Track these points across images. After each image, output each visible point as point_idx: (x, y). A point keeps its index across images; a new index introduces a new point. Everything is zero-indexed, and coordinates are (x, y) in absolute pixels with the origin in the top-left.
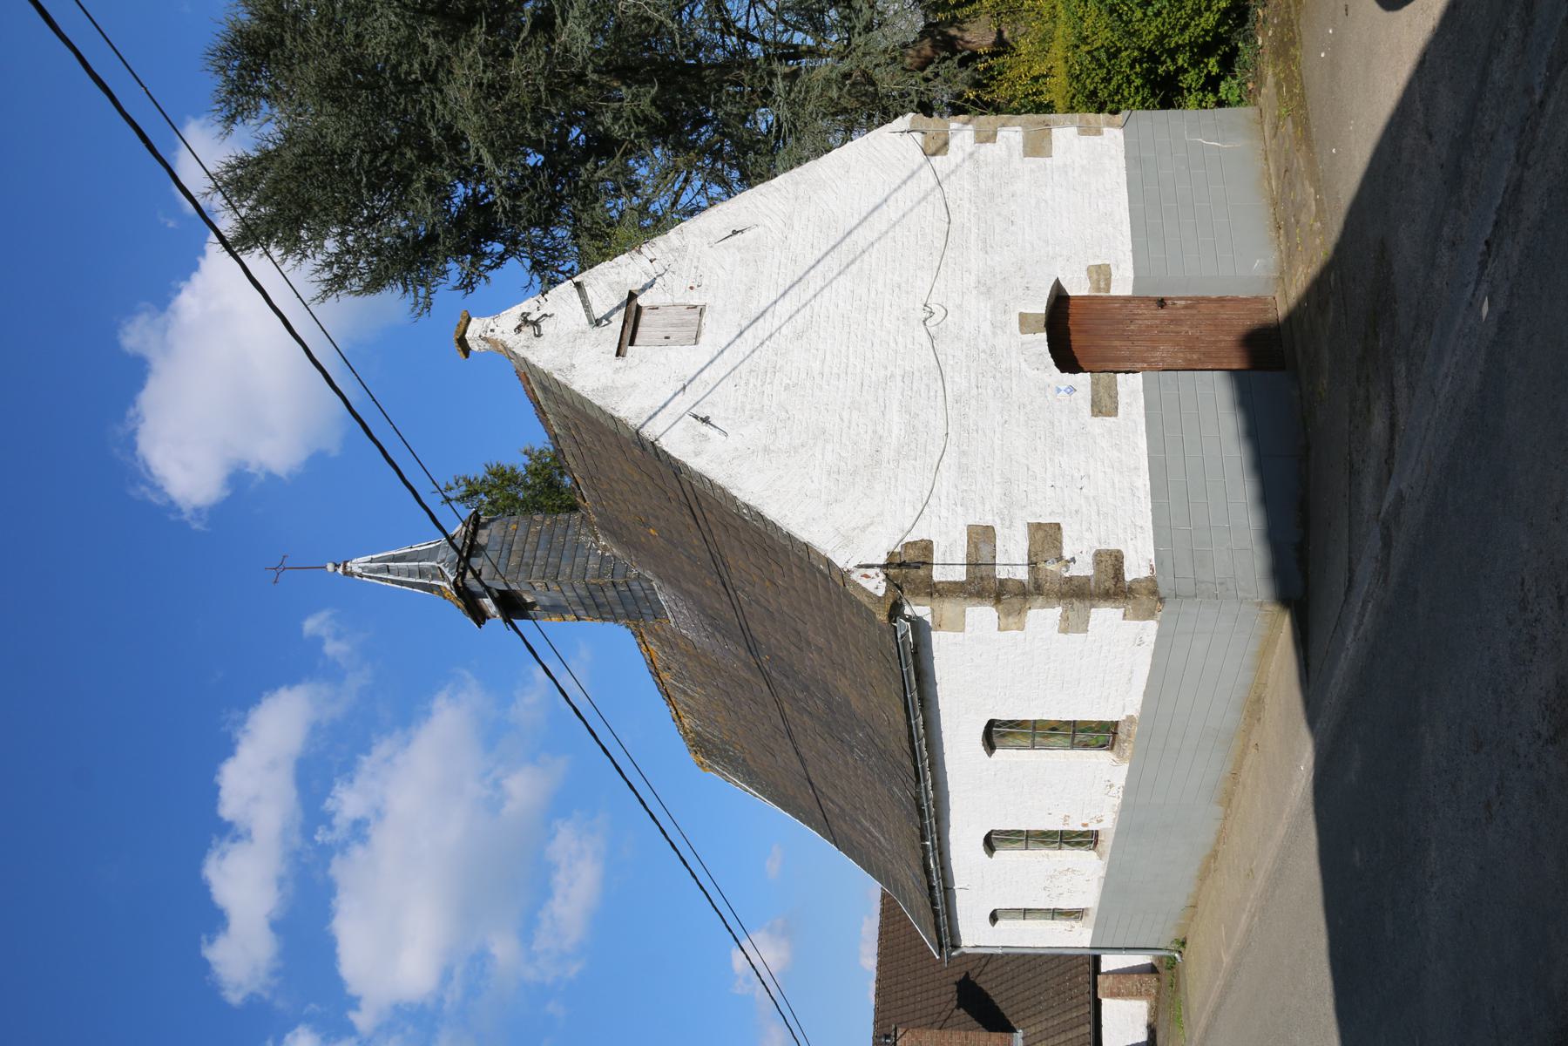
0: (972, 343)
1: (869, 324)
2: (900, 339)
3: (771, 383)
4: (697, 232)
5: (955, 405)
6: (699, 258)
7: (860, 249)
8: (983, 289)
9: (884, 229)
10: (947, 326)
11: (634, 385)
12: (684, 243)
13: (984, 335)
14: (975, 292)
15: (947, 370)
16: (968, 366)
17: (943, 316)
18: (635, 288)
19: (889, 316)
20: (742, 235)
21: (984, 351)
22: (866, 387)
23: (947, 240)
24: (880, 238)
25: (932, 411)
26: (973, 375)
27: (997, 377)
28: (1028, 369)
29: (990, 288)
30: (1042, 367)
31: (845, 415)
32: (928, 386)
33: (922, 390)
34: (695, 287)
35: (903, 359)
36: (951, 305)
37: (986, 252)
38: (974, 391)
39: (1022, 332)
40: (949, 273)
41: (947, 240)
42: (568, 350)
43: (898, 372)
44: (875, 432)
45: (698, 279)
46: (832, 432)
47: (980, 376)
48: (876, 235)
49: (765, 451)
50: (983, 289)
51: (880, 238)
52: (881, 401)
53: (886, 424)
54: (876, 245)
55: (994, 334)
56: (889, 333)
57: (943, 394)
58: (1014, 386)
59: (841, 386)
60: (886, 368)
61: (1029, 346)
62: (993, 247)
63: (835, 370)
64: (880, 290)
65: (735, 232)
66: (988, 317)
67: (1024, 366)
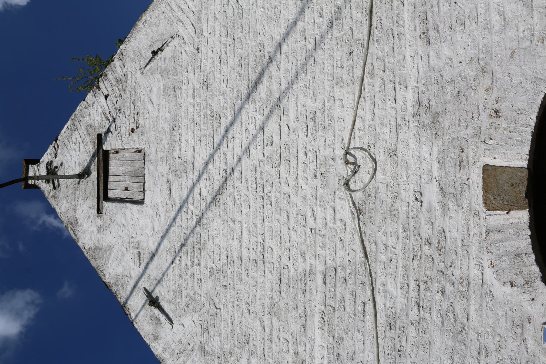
0: (412, 223)
1: (283, 184)
2: (319, 213)
3: (198, 264)
4: (131, 55)
5: (388, 334)
6: (135, 90)
7: (267, 55)
8: (426, 118)
9: (292, 17)
10: (377, 189)
11: (110, 248)
12: (124, 71)
13: (429, 211)
14: (413, 125)
15: (378, 268)
16: (405, 267)
17: (371, 171)
18: (102, 131)
19: (305, 171)
20: (163, 53)
21: (428, 242)
22: (284, 285)
23: (371, 26)
24: (288, 34)
25: (360, 337)
26: (412, 284)
27: (447, 292)
28: (495, 282)
29: (437, 114)
30: (520, 281)
31: (267, 323)
32: (353, 294)
33: (347, 300)
34: (135, 128)
35: (323, 247)
36: (382, 151)
37: (429, 42)
38: (414, 313)
39: (489, 205)
40: (377, 88)
41: (371, 26)
42: (73, 203)
43: (319, 267)
44: (297, 353)
45: (136, 118)
46: (255, 343)
47: (422, 286)
48: (283, 30)
49: (202, 350)
50: (426, 118)
51: (288, 34)
52: (301, 307)
53: (308, 345)
54: (285, 47)
55: (444, 207)
56: (306, 200)
57: (372, 310)
58: (472, 312)
59: (259, 280)
60: (304, 257)
61: (499, 236)
62: (436, 29)
63: (253, 256)
64: (292, 125)
65: (155, 53)
66: (435, 174)
67: (489, 273)
